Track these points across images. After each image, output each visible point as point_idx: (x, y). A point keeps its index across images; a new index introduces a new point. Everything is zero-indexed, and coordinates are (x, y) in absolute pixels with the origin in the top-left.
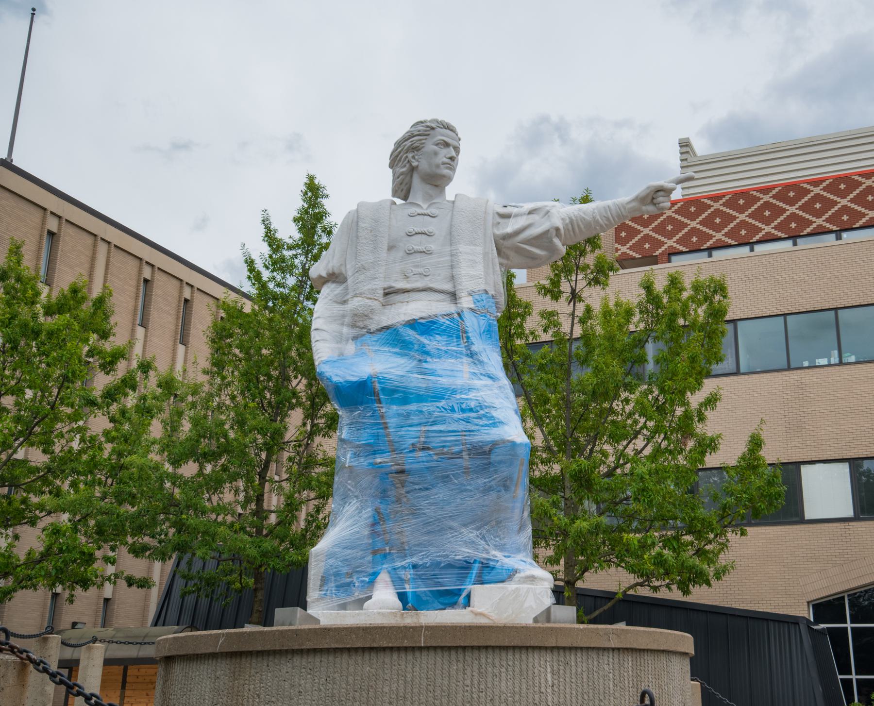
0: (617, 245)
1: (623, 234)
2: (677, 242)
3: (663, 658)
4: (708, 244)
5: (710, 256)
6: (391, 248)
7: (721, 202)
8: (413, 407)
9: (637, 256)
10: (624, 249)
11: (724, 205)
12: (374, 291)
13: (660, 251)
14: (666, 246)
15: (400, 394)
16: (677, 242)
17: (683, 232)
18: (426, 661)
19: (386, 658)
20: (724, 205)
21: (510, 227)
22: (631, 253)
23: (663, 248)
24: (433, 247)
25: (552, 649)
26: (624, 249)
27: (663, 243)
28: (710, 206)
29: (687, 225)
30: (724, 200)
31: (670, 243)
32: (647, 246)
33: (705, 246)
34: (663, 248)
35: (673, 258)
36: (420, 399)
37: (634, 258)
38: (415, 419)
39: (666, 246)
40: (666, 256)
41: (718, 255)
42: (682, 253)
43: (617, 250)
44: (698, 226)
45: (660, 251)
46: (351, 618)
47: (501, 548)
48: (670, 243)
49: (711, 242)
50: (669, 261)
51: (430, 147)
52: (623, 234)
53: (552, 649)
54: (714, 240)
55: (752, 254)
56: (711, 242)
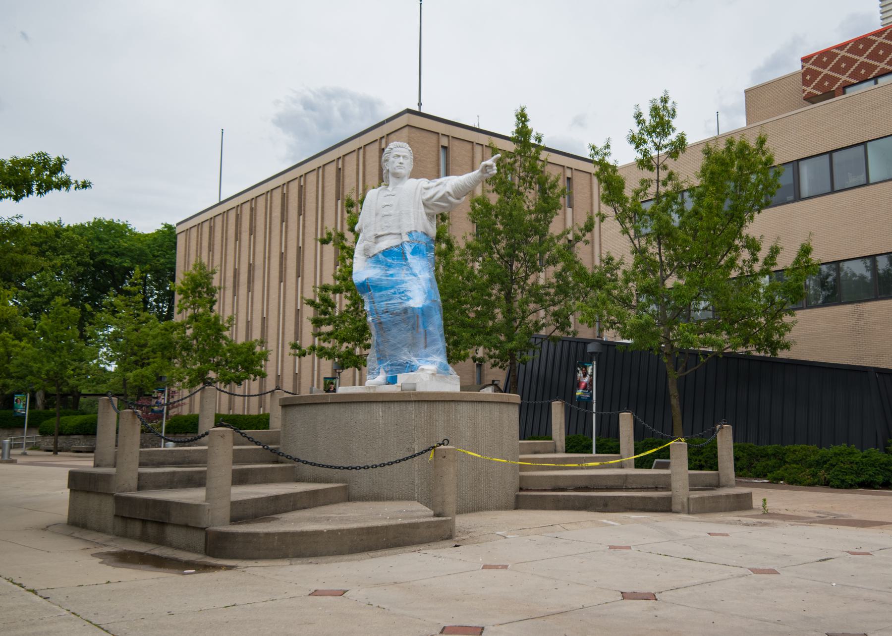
0: (804, 87)
1: (808, 77)
2: (850, 76)
3: (453, 405)
4: (874, 74)
5: (876, 83)
6: (377, 214)
7: (884, 36)
8: (384, 293)
9: (819, 93)
10: (809, 89)
11: (886, 38)
12: (370, 237)
13: (836, 86)
14: (841, 81)
15: (378, 288)
16: (850, 76)
17: (854, 67)
18: (332, 408)
19: (320, 407)
20: (886, 38)
21: (430, 193)
22: (815, 92)
23: (839, 84)
24: (391, 212)
25: (382, 402)
26: (809, 89)
27: (839, 79)
28: (875, 41)
29: (857, 61)
30: (886, 34)
31: (844, 78)
32: (826, 84)
33: (871, 76)
34: (839, 84)
35: (848, 90)
36: (386, 289)
37: (817, 96)
38: (384, 299)
39: (841, 81)
40: (841, 90)
41: (882, 81)
42: (853, 85)
43: (804, 91)
44: (866, 60)
45: (836, 86)
46: (357, 389)
47: (416, 356)
48: (844, 78)
49: (876, 71)
50: (844, 93)
51: (392, 159)
52: (808, 77)
53: (382, 402)
54: (878, 69)
55: (877, 86)
56: (876, 71)
